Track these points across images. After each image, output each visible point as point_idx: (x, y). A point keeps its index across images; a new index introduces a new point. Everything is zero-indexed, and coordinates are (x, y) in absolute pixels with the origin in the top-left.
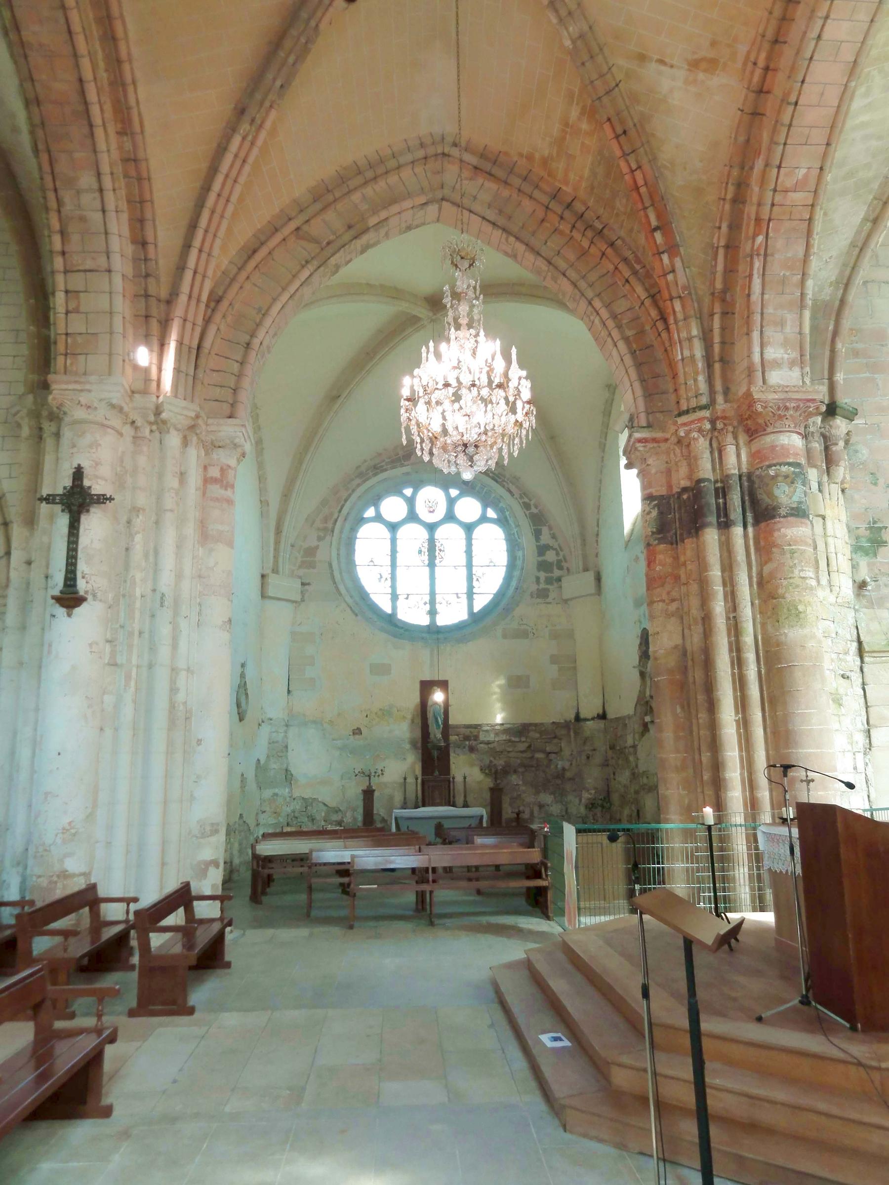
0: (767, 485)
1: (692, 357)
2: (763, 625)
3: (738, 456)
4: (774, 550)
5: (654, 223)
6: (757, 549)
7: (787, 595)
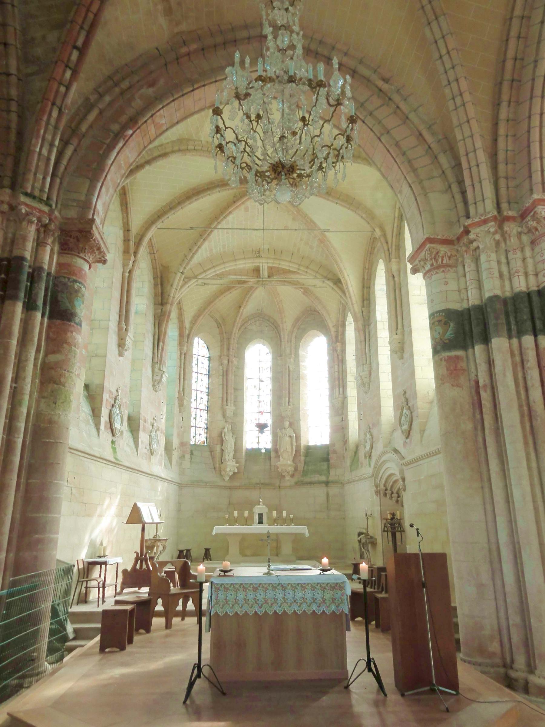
0: (71, 294)
1: (48, 159)
2: (38, 402)
3: (51, 258)
4: (65, 345)
5: (80, 43)
6: (48, 337)
7: (67, 385)
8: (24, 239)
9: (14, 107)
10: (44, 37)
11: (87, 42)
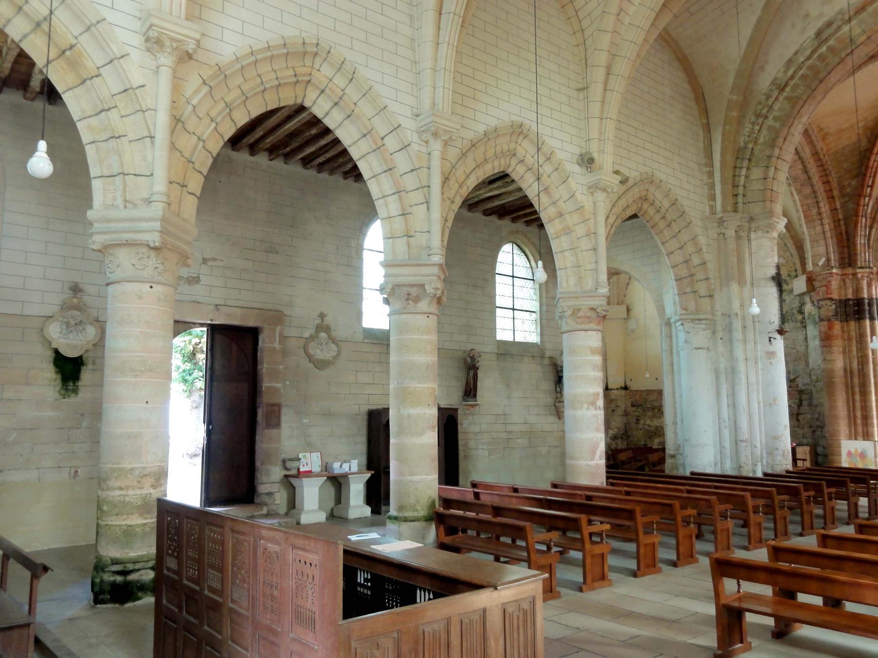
5: (870, 184)
8: (862, 288)
9: (842, 223)
10: (850, 184)
11: (873, 182)
